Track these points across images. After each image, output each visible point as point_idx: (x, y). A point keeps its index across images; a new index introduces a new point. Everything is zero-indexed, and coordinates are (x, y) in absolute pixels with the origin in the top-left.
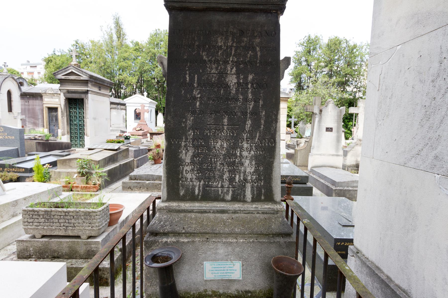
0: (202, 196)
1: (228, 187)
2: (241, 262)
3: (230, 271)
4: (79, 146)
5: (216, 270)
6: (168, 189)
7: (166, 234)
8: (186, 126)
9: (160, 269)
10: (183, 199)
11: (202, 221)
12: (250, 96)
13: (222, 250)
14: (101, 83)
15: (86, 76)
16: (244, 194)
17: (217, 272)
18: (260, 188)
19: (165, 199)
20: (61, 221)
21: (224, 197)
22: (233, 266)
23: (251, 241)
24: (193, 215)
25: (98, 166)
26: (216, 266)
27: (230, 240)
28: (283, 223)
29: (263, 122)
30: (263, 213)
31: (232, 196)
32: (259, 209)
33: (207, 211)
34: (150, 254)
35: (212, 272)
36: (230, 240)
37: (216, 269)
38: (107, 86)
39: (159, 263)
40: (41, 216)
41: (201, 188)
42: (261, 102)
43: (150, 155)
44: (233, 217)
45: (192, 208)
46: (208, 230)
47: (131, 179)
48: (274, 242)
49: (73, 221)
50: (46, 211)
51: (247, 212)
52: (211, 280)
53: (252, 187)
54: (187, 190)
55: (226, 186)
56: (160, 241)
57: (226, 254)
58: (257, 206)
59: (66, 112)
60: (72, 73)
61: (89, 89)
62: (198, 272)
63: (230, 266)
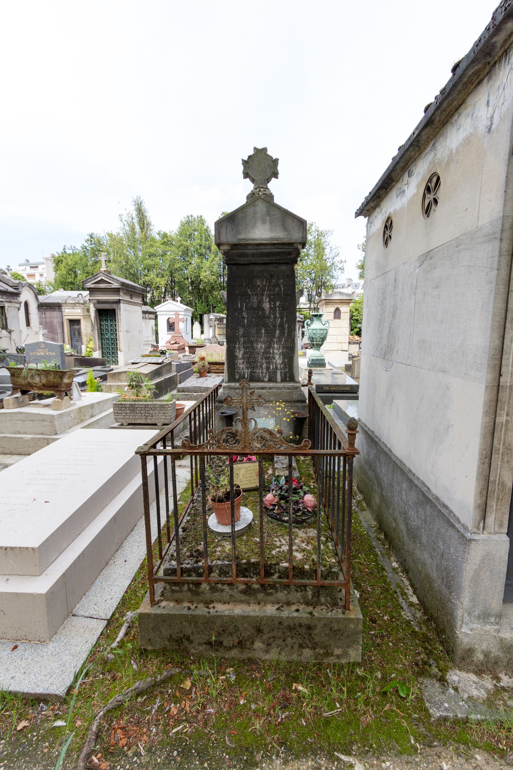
4: (111, 362)
8: (239, 335)
12: (278, 315)
14: (132, 290)
15: (118, 283)
20: (142, 412)
25: (147, 379)
29: (286, 331)
38: (139, 293)
40: (128, 409)
42: (285, 319)
43: (195, 368)
47: (179, 391)
49: (151, 412)
50: (131, 405)
53: (281, 373)
54: (240, 375)
59: (97, 325)
60: (102, 281)
61: (121, 298)
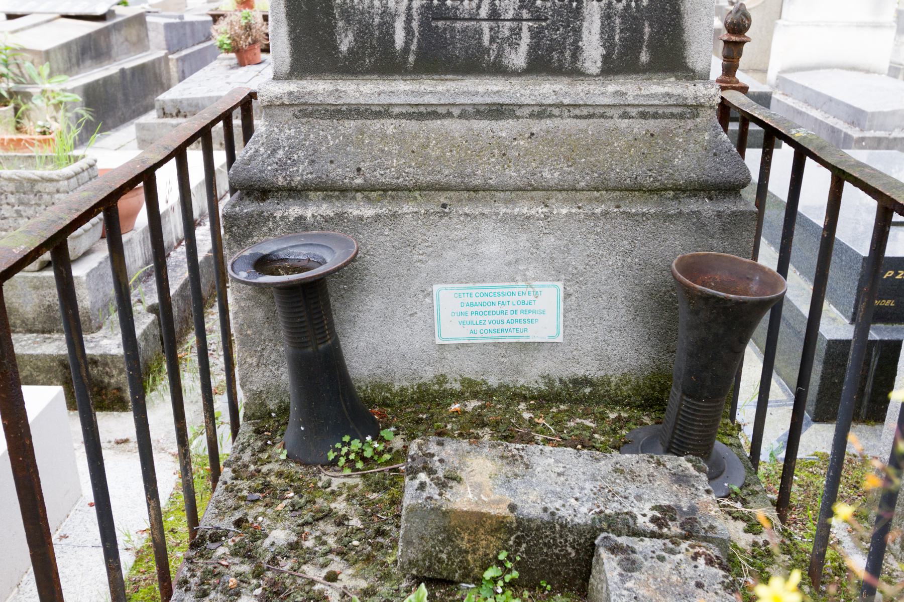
0: (422, 54)
1: (518, 19)
2: (560, 285)
3: (523, 316)
5: (477, 313)
6: (292, 31)
7: (296, 192)
9: (287, 289)
10: (350, 67)
11: (425, 146)
13: (494, 244)
16: (576, 42)
17: (479, 318)
18: (635, 18)
19: (286, 68)
21: (500, 55)
22: (532, 298)
23: (598, 211)
24: (390, 126)
25: (45, 70)
26: (474, 300)
27: (525, 210)
28: (714, 150)
30: (643, 116)
31: (529, 54)
32: (630, 100)
33: (441, 110)
34: (247, 253)
35: (462, 318)
36: (524, 208)
37: (475, 309)
39: (280, 275)
41: (415, 24)
43: (221, 33)
44: (534, 130)
45: (384, 100)
46: (446, 175)
48: (680, 213)
51: (585, 112)
52: (458, 347)
53: (607, 17)
54: (363, 32)
55: (510, 15)
56: (278, 214)
57: (510, 257)
58: (623, 89)
62: (414, 319)
63: (522, 298)
